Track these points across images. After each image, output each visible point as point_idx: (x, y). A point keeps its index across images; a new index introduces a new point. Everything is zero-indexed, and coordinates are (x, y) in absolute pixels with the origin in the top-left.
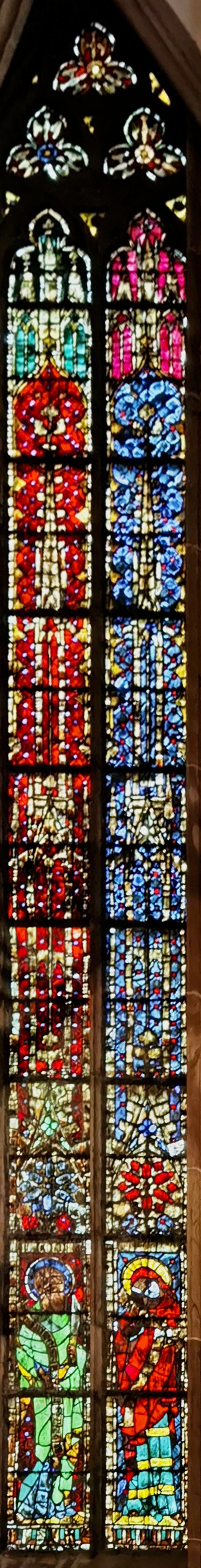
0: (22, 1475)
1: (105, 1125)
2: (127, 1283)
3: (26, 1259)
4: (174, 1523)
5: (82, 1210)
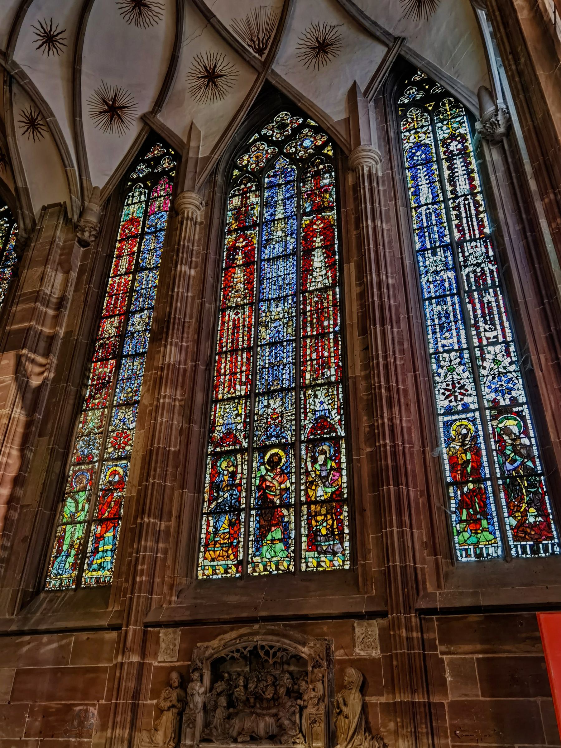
0: (56, 557)
1: (110, 421)
2: (107, 477)
3: (75, 472)
4: (109, 573)
5: (97, 452)
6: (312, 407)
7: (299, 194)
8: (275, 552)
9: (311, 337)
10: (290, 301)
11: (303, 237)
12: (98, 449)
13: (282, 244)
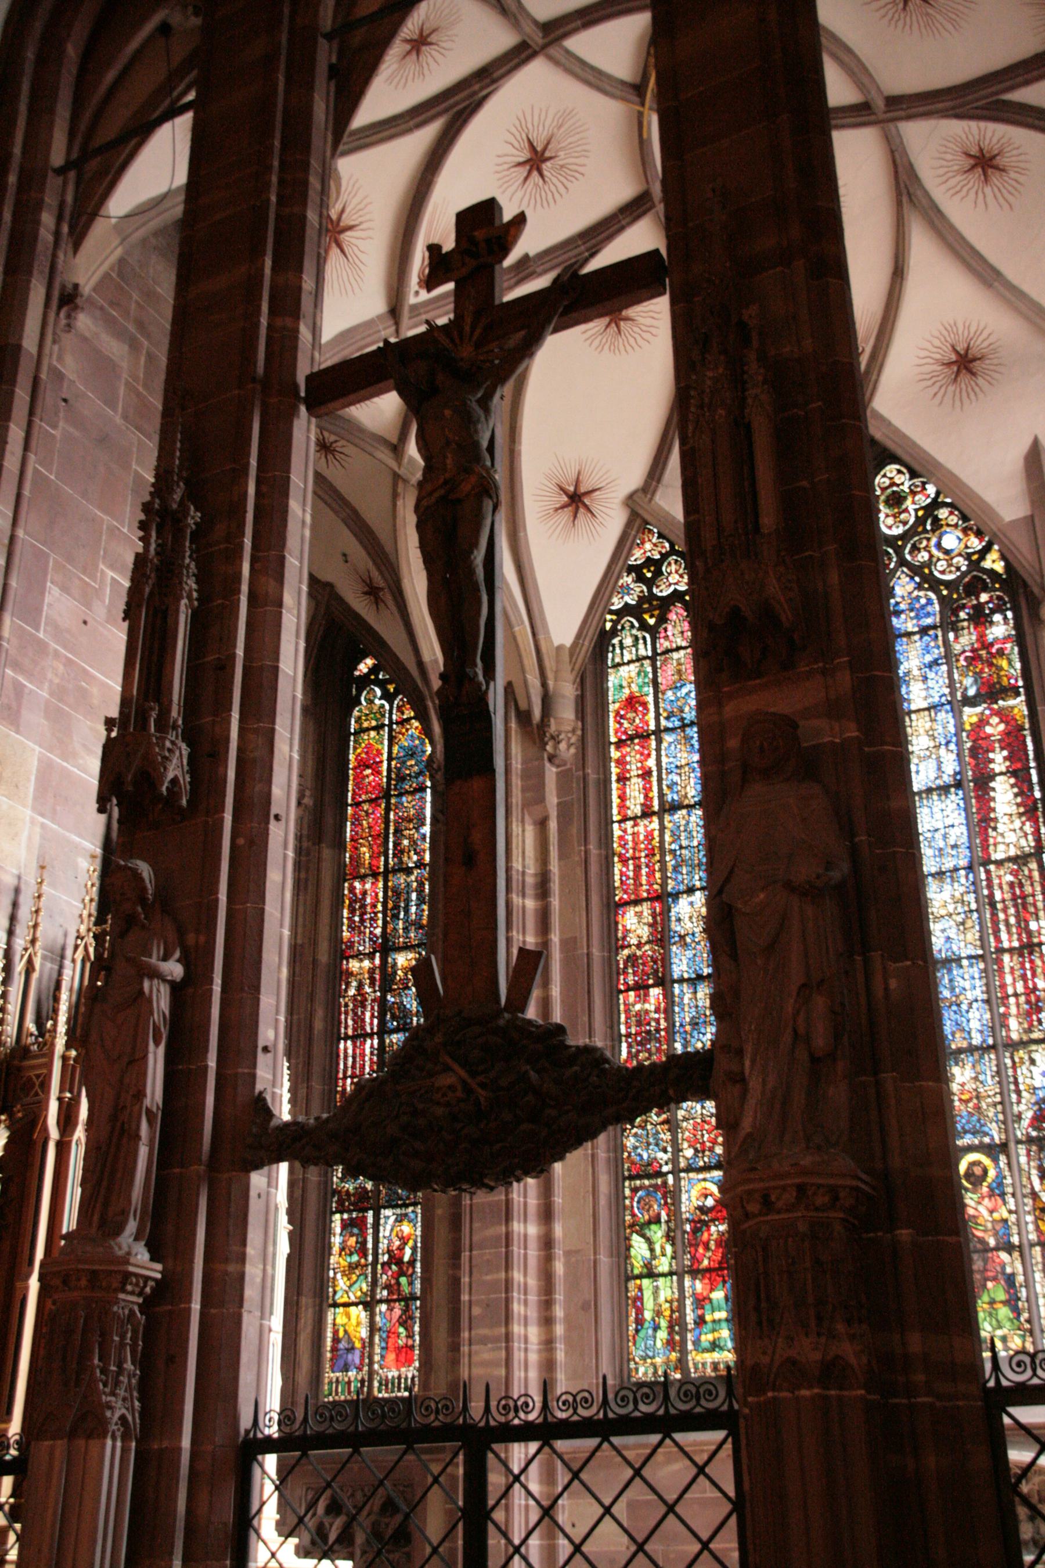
0: (637, 1331)
6: (1028, 1081)
7: (949, 657)
8: (997, 1320)
9: (1011, 950)
10: (963, 880)
11: (971, 749)
12: (665, 1151)
13: (932, 764)
